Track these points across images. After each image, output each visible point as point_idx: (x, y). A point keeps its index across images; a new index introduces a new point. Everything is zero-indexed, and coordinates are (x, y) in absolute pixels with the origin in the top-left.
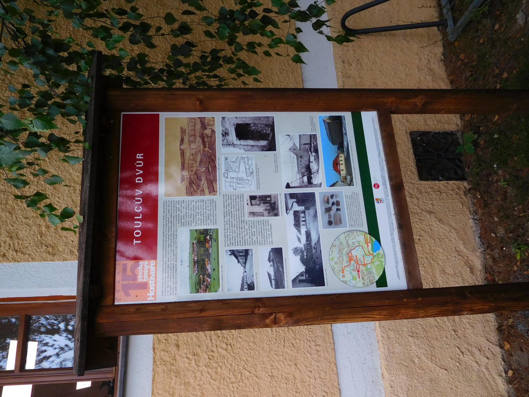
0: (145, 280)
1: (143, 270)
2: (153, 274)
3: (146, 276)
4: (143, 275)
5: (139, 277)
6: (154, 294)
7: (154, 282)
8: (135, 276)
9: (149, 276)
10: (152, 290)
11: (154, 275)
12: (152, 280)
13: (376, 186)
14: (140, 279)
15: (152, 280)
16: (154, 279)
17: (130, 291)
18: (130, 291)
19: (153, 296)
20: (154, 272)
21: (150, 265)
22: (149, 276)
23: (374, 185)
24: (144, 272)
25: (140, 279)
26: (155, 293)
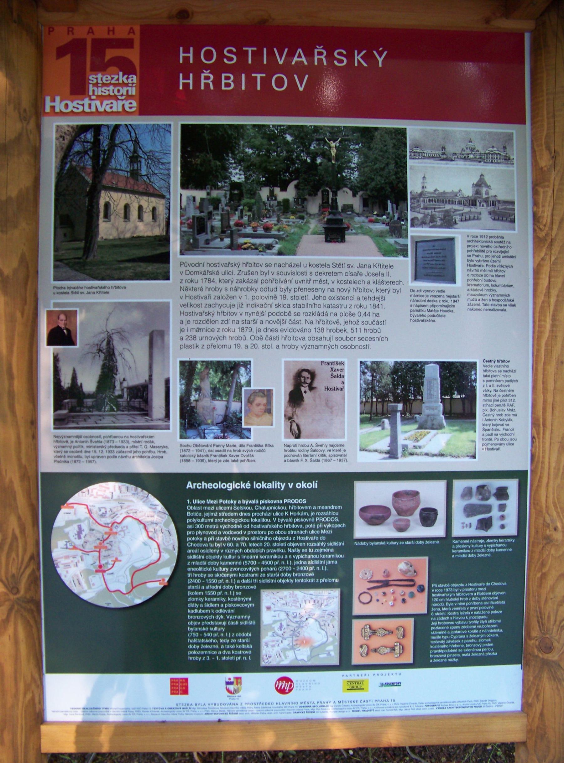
0: (91, 88)
1: (115, 85)
2: (105, 106)
3: (99, 91)
4: (104, 85)
5: (100, 76)
6: (57, 110)
7: (87, 110)
9: (101, 98)
10: (67, 106)
11: (101, 109)
12: (90, 105)
13: (283, 684)
15: (90, 105)
16: (93, 109)
17: (68, 58)
18: (68, 58)
19: (53, 108)
20: (108, 110)
21: (126, 99)
22: (101, 98)
23: (288, 680)
24: (111, 88)
25: (92, 78)
26: (62, 113)
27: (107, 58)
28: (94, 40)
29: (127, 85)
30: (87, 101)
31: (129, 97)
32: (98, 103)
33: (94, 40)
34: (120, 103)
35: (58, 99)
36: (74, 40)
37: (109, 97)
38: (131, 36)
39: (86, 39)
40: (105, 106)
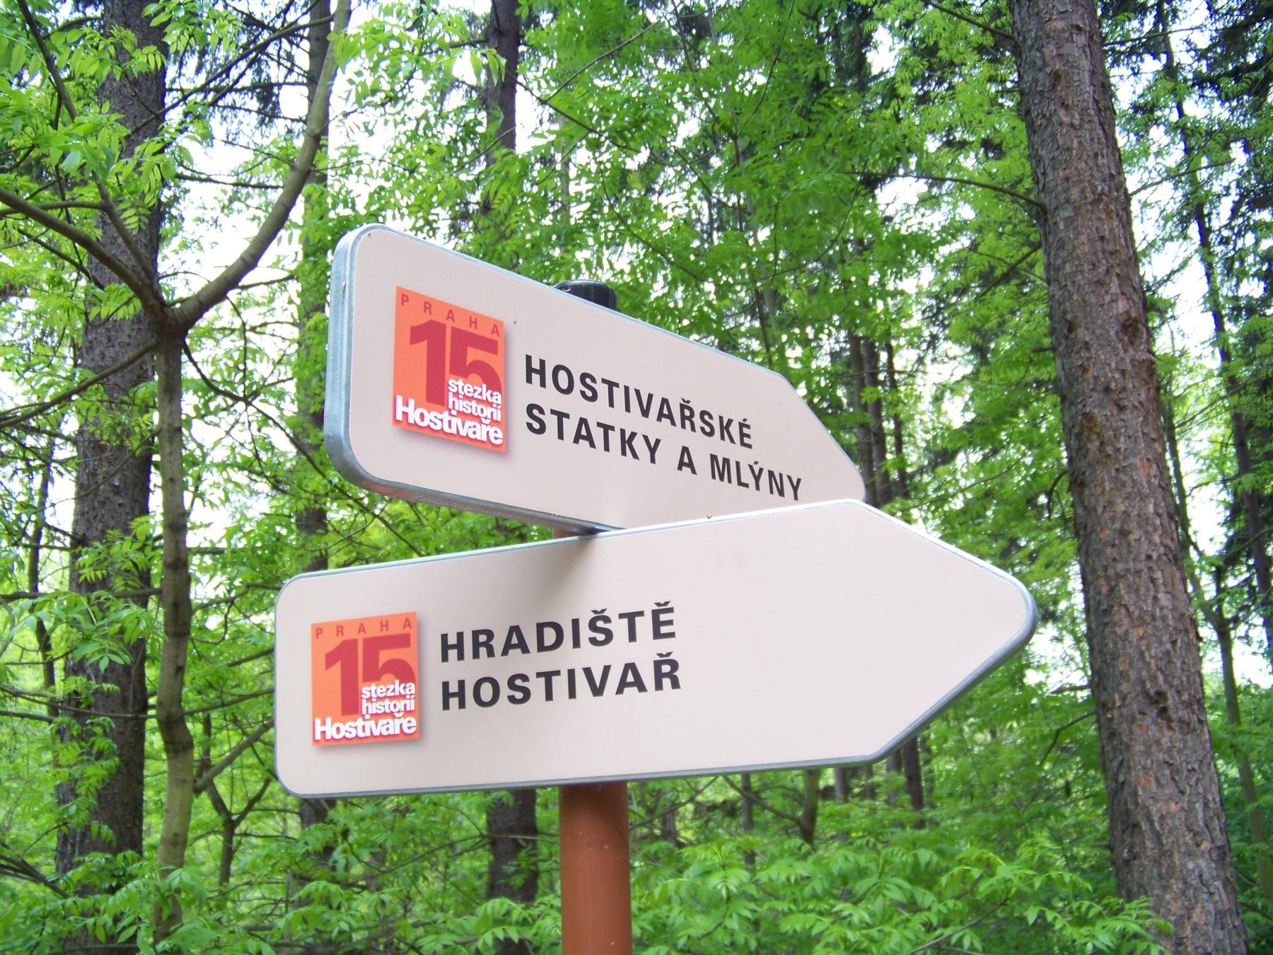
0: (364, 704)
1: (391, 698)
3: (374, 708)
4: (379, 699)
5: (373, 687)
7: (361, 734)
8: (374, 675)
9: (376, 716)
11: (376, 733)
14: (368, 690)
19: (323, 733)
24: (387, 702)
25: (368, 690)
27: (381, 664)
28: (365, 641)
29: (404, 697)
30: (360, 722)
31: (407, 713)
32: (372, 723)
33: (365, 641)
34: (398, 722)
35: (328, 720)
36: (345, 643)
37: (385, 714)
38: (407, 630)
39: (355, 641)
40: (381, 728)
